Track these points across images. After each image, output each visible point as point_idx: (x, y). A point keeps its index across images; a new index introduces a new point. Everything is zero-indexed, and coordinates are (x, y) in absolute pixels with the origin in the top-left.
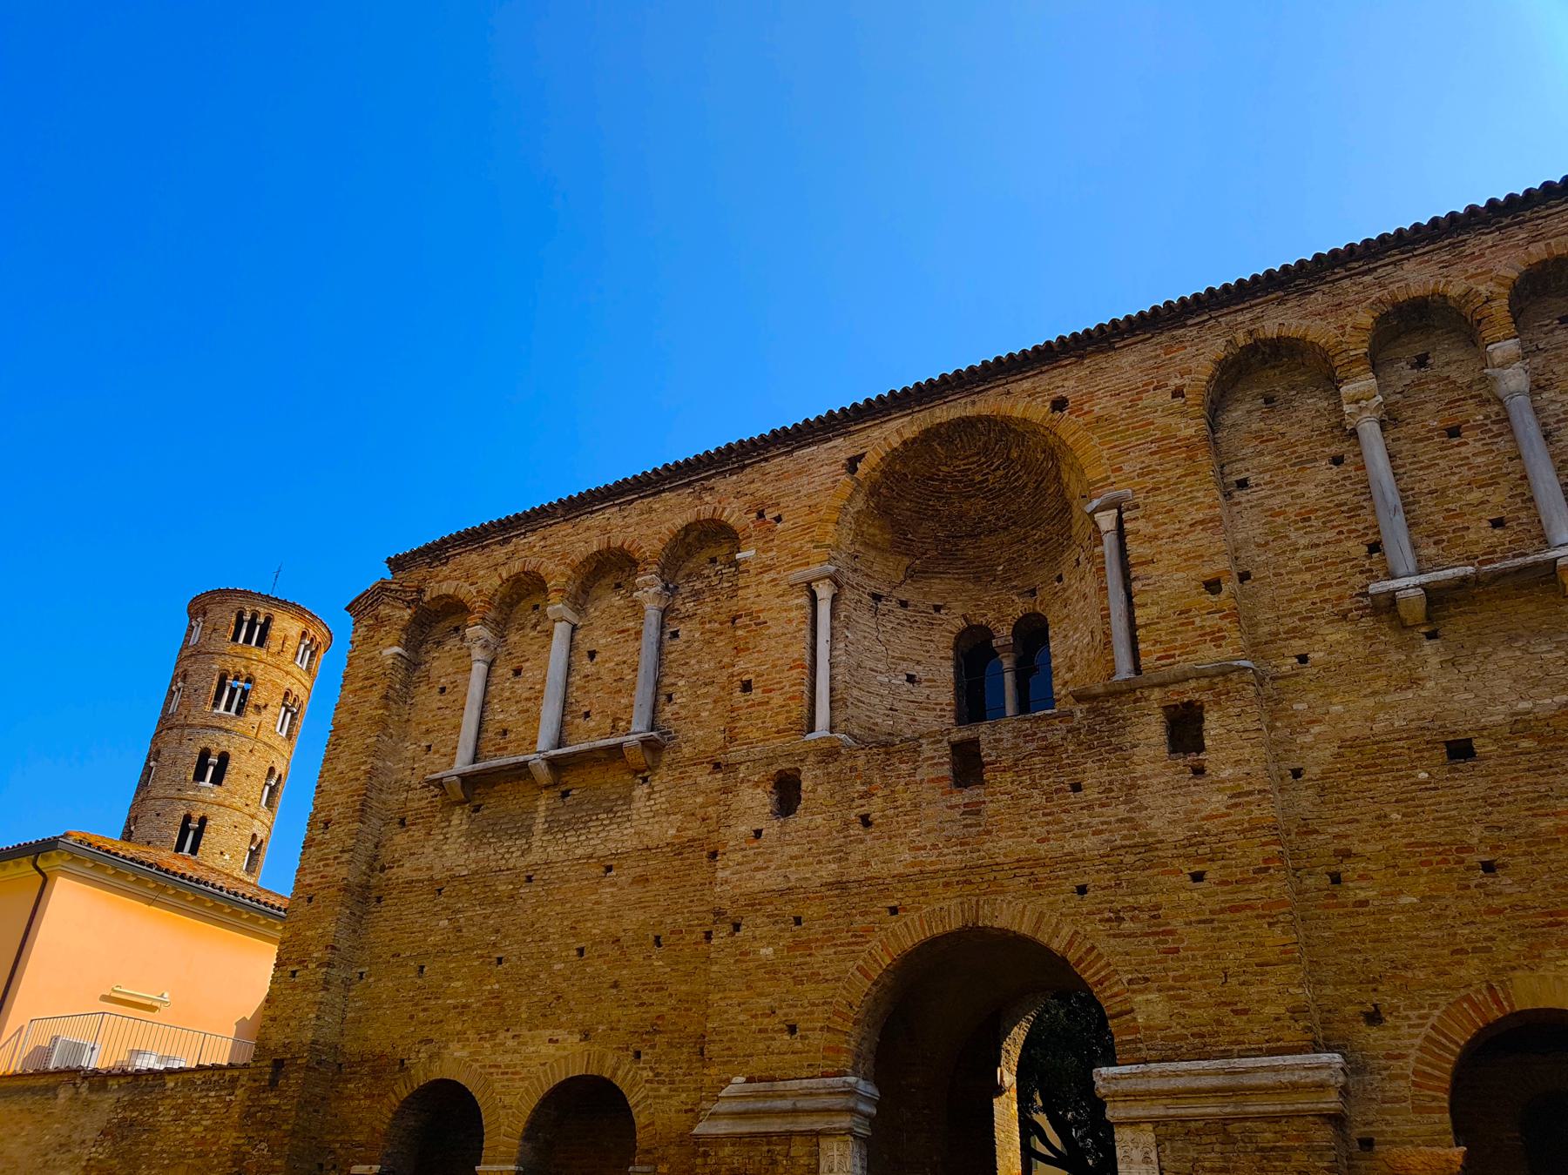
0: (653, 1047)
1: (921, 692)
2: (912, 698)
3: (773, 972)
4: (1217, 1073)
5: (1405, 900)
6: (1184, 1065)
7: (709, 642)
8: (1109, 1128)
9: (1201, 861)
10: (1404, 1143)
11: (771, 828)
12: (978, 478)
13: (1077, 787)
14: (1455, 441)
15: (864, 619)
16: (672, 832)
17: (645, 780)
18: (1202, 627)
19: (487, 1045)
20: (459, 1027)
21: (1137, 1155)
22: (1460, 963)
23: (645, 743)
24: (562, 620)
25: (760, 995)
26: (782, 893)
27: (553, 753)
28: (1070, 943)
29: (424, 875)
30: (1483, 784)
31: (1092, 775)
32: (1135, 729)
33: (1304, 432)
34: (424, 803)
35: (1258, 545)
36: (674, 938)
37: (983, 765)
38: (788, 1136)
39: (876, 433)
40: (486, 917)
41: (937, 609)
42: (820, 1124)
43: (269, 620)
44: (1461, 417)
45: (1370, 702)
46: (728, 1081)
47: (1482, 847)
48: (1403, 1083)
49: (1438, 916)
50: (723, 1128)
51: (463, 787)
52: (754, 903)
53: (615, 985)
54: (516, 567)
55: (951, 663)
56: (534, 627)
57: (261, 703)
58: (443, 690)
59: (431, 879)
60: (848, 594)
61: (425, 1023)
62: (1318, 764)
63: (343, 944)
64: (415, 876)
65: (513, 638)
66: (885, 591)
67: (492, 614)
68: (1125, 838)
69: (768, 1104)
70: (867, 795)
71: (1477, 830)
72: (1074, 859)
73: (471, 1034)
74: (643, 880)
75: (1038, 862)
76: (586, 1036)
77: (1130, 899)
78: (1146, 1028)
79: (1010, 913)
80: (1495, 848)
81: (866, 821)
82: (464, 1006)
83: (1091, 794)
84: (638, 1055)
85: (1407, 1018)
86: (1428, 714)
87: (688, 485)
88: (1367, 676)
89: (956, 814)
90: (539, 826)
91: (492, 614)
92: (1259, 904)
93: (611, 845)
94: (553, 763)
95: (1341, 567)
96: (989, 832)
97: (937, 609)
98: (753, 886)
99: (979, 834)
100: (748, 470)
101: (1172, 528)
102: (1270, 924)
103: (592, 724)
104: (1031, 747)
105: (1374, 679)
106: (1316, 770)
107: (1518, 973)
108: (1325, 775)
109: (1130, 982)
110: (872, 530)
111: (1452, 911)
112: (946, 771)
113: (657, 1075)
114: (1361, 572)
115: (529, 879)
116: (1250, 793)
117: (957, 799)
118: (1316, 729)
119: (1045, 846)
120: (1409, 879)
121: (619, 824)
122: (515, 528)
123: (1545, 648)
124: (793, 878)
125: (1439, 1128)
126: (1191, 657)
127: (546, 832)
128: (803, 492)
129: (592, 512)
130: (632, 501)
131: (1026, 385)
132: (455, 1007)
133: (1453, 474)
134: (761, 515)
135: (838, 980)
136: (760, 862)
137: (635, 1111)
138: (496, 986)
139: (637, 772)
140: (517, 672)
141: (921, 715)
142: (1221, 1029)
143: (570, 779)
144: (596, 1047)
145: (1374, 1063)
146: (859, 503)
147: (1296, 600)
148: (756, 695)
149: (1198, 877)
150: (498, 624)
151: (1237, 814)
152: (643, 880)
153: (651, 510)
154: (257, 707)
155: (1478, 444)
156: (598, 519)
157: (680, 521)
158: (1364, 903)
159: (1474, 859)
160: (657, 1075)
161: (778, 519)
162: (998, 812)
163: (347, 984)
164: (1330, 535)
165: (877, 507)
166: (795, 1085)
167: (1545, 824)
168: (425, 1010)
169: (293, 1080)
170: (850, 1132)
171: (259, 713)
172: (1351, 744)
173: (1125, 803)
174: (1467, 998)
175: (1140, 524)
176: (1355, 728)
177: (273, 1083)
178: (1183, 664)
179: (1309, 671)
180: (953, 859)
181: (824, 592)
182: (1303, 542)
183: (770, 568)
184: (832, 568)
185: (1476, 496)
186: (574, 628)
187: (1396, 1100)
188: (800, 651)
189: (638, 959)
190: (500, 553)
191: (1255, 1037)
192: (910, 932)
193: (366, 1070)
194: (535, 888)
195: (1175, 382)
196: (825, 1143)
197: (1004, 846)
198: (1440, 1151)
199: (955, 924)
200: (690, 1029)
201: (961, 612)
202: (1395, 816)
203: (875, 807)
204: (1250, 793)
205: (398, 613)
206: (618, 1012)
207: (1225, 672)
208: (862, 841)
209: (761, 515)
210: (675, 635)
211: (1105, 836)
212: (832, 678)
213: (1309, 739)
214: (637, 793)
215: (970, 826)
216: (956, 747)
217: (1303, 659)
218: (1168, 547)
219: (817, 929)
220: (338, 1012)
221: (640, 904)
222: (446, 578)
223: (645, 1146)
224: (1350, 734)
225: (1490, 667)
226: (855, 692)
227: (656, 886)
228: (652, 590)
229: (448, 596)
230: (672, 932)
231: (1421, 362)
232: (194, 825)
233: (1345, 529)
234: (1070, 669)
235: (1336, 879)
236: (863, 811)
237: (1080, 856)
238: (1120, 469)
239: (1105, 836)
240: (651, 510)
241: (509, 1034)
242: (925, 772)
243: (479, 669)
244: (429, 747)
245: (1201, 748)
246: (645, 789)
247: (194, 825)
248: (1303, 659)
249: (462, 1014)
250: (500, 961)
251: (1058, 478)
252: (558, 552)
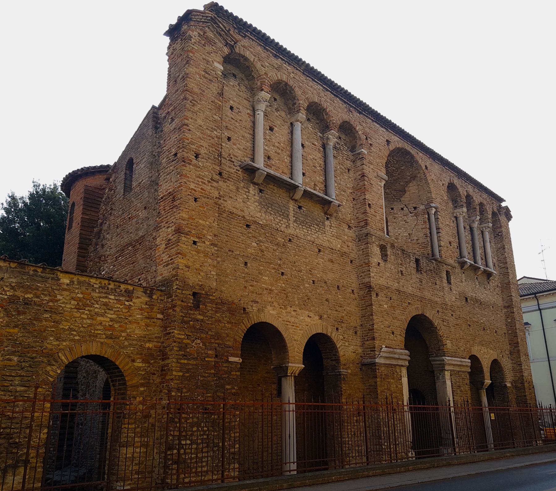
0: (342, 327)
6: (456, 359)
19: (283, 311)
20: (270, 299)
25: (386, 320)
36: (343, 288)
50: (382, 361)
61: (253, 292)
69: (392, 356)
76: (321, 317)
82: (270, 290)
84: (337, 329)
100: (362, 115)
113: (344, 338)
130: (327, 90)
132: (266, 289)
138: (283, 285)
160: (344, 338)
166: (398, 351)
168: (252, 286)
193: (225, 308)
200: (351, 324)
203: (403, 269)
223: (343, 363)
229: (246, 59)
234: (396, 239)
241: (292, 309)
249: (270, 293)
251: (407, 183)
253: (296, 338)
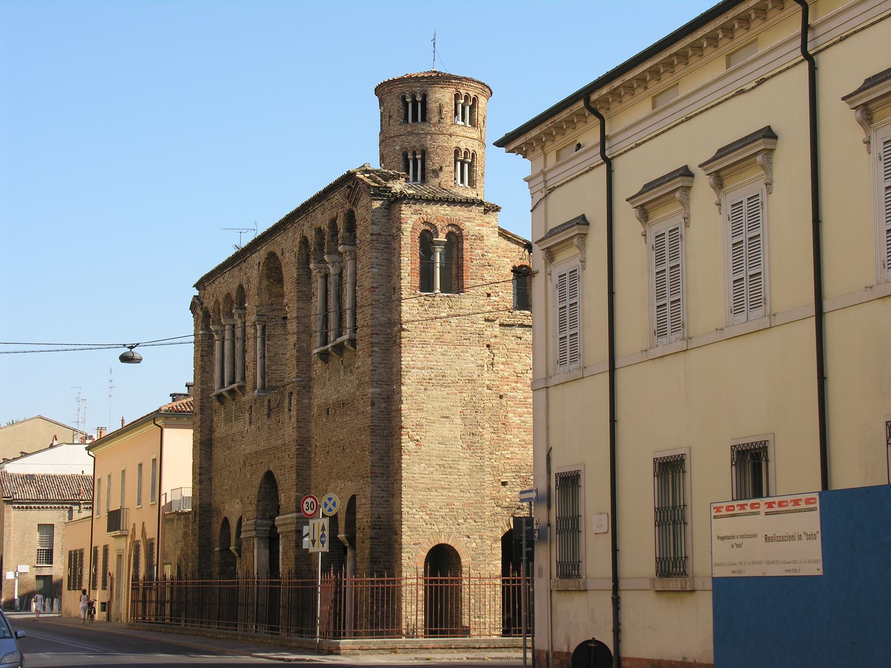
43: (424, 96)
57: (437, 167)
146: (265, 283)
154: (434, 171)
163: (210, 480)
165: (274, 280)
171: (437, 176)
226: (274, 367)
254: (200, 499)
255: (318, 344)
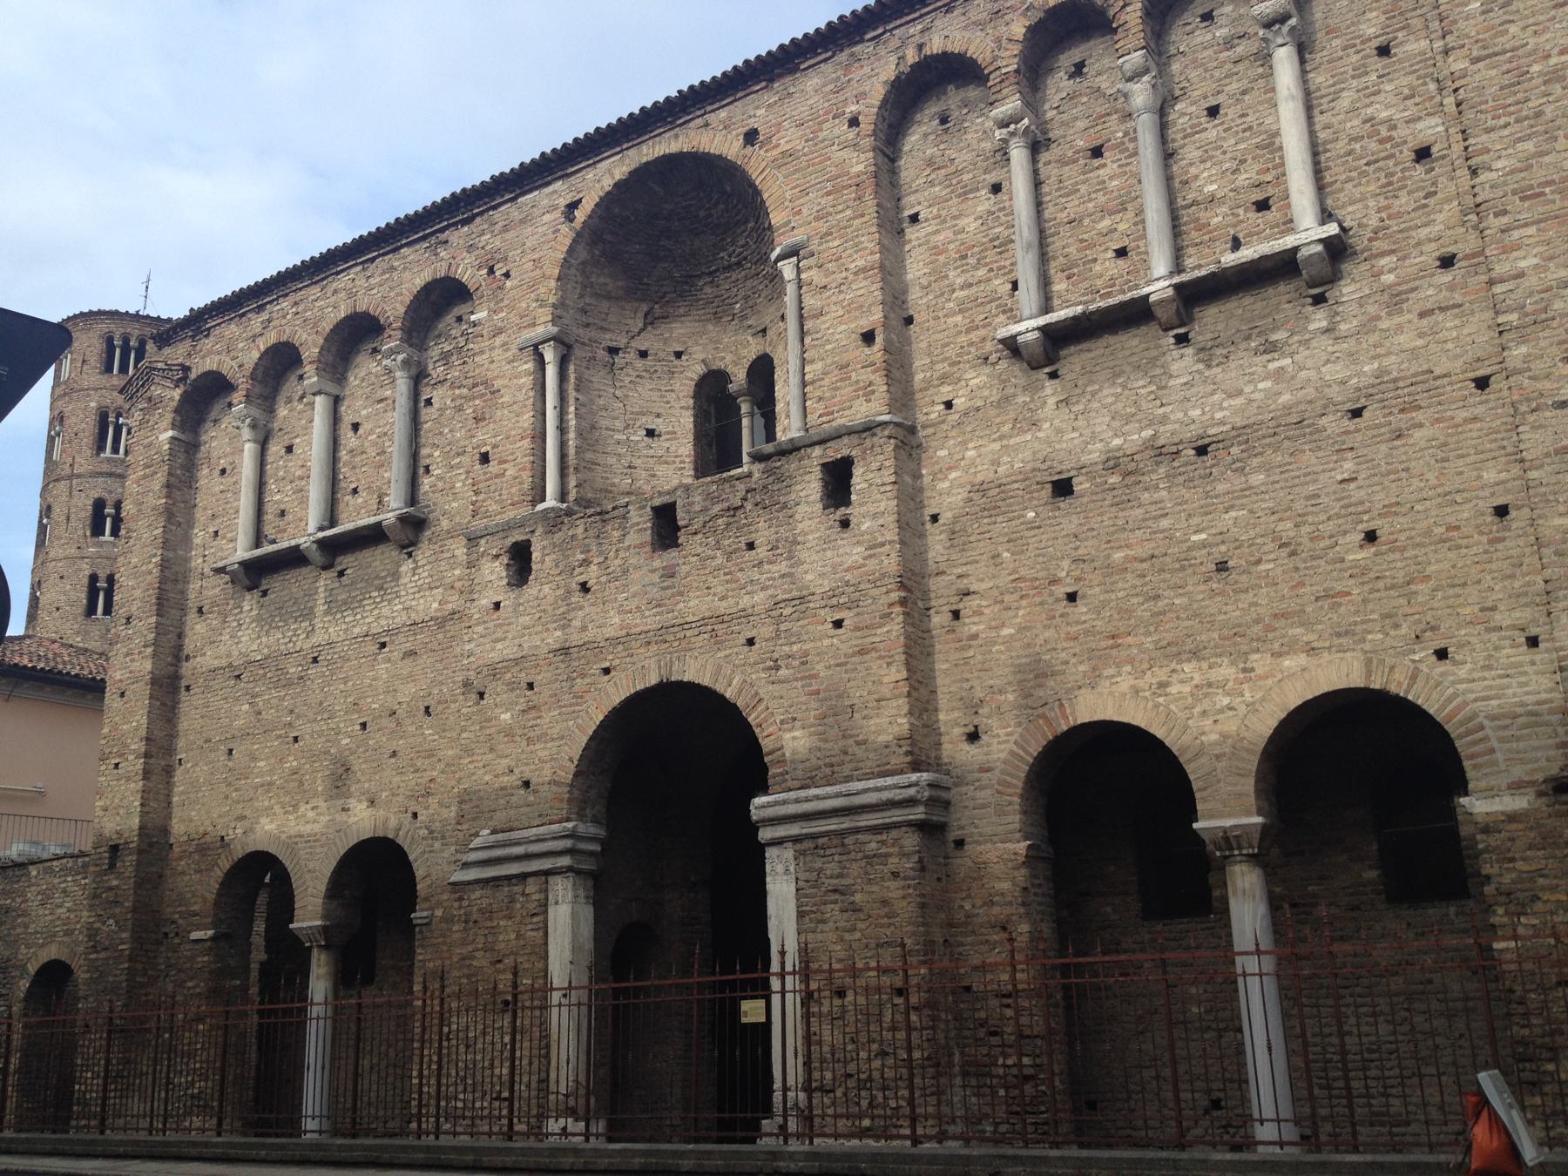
0: (427, 808)
1: (659, 446)
2: (651, 452)
3: (509, 733)
4: (837, 795)
5: (1006, 632)
7: (460, 409)
8: (760, 850)
9: (841, 610)
10: (986, 842)
11: (508, 599)
12: (702, 214)
13: (751, 546)
14: (1096, 162)
15: (598, 378)
16: (435, 605)
17: (410, 555)
18: (857, 382)
21: (780, 868)
22: (1040, 686)
23: (403, 520)
24: (319, 393)
26: (517, 661)
27: (321, 535)
28: (740, 691)
29: (224, 663)
30: (1075, 519)
31: (763, 533)
32: (799, 487)
33: (969, 157)
34: (216, 591)
35: (924, 288)
37: (679, 529)
38: (523, 877)
39: (590, 175)
40: (282, 699)
41: (678, 355)
42: (546, 864)
44: (1105, 135)
45: (996, 446)
46: (477, 835)
47: (1068, 580)
48: (989, 792)
49: (1029, 645)
51: (246, 574)
52: (494, 671)
53: (394, 754)
54: (272, 338)
55: (691, 412)
56: (302, 397)
58: (223, 471)
59: (230, 665)
60: (578, 352)
62: (951, 509)
63: (158, 734)
64: (216, 663)
65: (282, 412)
66: (621, 341)
67: (258, 390)
68: (785, 591)
70: (586, 563)
71: (1065, 564)
72: (745, 615)
73: (277, 808)
74: (412, 654)
75: (720, 618)
76: (372, 802)
77: (786, 648)
78: (793, 761)
79: (694, 670)
80: (1078, 580)
81: (585, 588)
82: (270, 784)
83: (761, 552)
85: (998, 736)
86: (1040, 456)
87: (424, 238)
88: (998, 420)
89: (656, 578)
90: (321, 608)
91: (258, 390)
92: (881, 646)
93: (383, 622)
94: (323, 544)
95: (988, 307)
96: (681, 594)
97: (678, 355)
98: (494, 656)
99: (673, 595)
100: (478, 220)
101: (839, 277)
102: (888, 664)
103: (360, 500)
104: (716, 509)
105: (1003, 423)
106: (949, 515)
107: (1083, 691)
108: (956, 519)
109: (782, 722)
110: (602, 280)
111: (1040, 641)
112: (647, 536)
114: (1004, 312)
115: (315, 660)
116: (883, 544)
117: (657, 563)
118: (953, 475)
119: (724, 604)
120: (1011, 613)
121: (389, 601)
122: (266, 295)
123: (1141, 383)
124: (526, 646)
125: (1011, 827)
126: (847, 413)
127: (327, 613)
128: (529, 244)
129: (338, 273)
130: (373, 260)
131: (723, 114)
133: (1091, 200)
134: (491, 271)
135: (562, 738)
136: (499, 634)
137: (415, 866)
139: (404, 547)
140: (289, 449)
141: (661, 470)
142: (848, 758)
143: (346, 561)
144: (382, 812)
145: (970, 778)
146: (583, 254)
147: (947, 345)
148: (493, 467)
149: (838, 624)
150: (266, 398)
151: (872, 564)
152: (412, 654)
153: (393, 269)
155: (1115, 166)
156: (343, 281)
157: (419, 281)
158: (975, 637)
159: (1061, 591)
160: (431, 832)
161: (507, 275)
162: (688, 574)
164: (982, 272)
167: (1118, 556)
168: (236, 790)
169: (128, 862)
170: (570, 869)
172: (981, 489)
173: (790, 558)
174: (1043, 716)
175: (813, 272)
176: (984, 474)
177: (112, 866)
178: (841, 421)
179: (953, 417)
180: (652, 620)
181: (549, 355)
182: (959, 281)
183: (500, 331)
184: (555, 330)
185: (1105, 223)
186: (337, 401)
187: (983, 806)
188: (527, 419)
189: (412, 729)
190: (256, 322)
191: (869, 764)
192: (617, 691)
194: (320, 668)
195: (852, 108)
196: (551, 880)
197: (695, 605)
198: (1009, 846)
199: (653, 680)
201: (702, 356)
202: (1006, 554)
203: (592, 574)
204: (883, 544)
205: (168, 393)
206: (397, 779)
207: (869, 428)
208: (581, 608)
209: (491, 271)
210: (429, 402)
211: (770, 592)
212: (563, 445)
213: (946, 484)
214: (403, 569)
215: (667, 588)
216: (655, 509)
217: (949, 405)
218: (834, 299)
219: (547, 693)
220: (161, 798)
221: (411, 677)
222: (210, 352)
224: (980, 478)
225: (1095, 405)
226: (589, 456)
227: (425, 660)
228: (400, 357)
230: (439, 702)
231: (1078, 70)
232: (102, 584)
233: (994, 266)
235: (956, 615)
236: (582, 579)
237: (750, 611)
238: (799, 212)
239: (770, 592)
240: (393, 269)
242: (632, 538)
243: (249, 449)
244: (216, 533)
245: (847, 503)
246: (410, 564)
247: (102, 584)
248: (949, 405)
250: (296, 739)
252: (308, 320)
253: (311, 865)
254: (143, 814)
255: (1034, 311)
